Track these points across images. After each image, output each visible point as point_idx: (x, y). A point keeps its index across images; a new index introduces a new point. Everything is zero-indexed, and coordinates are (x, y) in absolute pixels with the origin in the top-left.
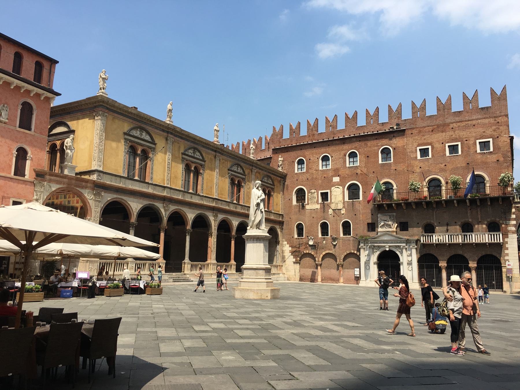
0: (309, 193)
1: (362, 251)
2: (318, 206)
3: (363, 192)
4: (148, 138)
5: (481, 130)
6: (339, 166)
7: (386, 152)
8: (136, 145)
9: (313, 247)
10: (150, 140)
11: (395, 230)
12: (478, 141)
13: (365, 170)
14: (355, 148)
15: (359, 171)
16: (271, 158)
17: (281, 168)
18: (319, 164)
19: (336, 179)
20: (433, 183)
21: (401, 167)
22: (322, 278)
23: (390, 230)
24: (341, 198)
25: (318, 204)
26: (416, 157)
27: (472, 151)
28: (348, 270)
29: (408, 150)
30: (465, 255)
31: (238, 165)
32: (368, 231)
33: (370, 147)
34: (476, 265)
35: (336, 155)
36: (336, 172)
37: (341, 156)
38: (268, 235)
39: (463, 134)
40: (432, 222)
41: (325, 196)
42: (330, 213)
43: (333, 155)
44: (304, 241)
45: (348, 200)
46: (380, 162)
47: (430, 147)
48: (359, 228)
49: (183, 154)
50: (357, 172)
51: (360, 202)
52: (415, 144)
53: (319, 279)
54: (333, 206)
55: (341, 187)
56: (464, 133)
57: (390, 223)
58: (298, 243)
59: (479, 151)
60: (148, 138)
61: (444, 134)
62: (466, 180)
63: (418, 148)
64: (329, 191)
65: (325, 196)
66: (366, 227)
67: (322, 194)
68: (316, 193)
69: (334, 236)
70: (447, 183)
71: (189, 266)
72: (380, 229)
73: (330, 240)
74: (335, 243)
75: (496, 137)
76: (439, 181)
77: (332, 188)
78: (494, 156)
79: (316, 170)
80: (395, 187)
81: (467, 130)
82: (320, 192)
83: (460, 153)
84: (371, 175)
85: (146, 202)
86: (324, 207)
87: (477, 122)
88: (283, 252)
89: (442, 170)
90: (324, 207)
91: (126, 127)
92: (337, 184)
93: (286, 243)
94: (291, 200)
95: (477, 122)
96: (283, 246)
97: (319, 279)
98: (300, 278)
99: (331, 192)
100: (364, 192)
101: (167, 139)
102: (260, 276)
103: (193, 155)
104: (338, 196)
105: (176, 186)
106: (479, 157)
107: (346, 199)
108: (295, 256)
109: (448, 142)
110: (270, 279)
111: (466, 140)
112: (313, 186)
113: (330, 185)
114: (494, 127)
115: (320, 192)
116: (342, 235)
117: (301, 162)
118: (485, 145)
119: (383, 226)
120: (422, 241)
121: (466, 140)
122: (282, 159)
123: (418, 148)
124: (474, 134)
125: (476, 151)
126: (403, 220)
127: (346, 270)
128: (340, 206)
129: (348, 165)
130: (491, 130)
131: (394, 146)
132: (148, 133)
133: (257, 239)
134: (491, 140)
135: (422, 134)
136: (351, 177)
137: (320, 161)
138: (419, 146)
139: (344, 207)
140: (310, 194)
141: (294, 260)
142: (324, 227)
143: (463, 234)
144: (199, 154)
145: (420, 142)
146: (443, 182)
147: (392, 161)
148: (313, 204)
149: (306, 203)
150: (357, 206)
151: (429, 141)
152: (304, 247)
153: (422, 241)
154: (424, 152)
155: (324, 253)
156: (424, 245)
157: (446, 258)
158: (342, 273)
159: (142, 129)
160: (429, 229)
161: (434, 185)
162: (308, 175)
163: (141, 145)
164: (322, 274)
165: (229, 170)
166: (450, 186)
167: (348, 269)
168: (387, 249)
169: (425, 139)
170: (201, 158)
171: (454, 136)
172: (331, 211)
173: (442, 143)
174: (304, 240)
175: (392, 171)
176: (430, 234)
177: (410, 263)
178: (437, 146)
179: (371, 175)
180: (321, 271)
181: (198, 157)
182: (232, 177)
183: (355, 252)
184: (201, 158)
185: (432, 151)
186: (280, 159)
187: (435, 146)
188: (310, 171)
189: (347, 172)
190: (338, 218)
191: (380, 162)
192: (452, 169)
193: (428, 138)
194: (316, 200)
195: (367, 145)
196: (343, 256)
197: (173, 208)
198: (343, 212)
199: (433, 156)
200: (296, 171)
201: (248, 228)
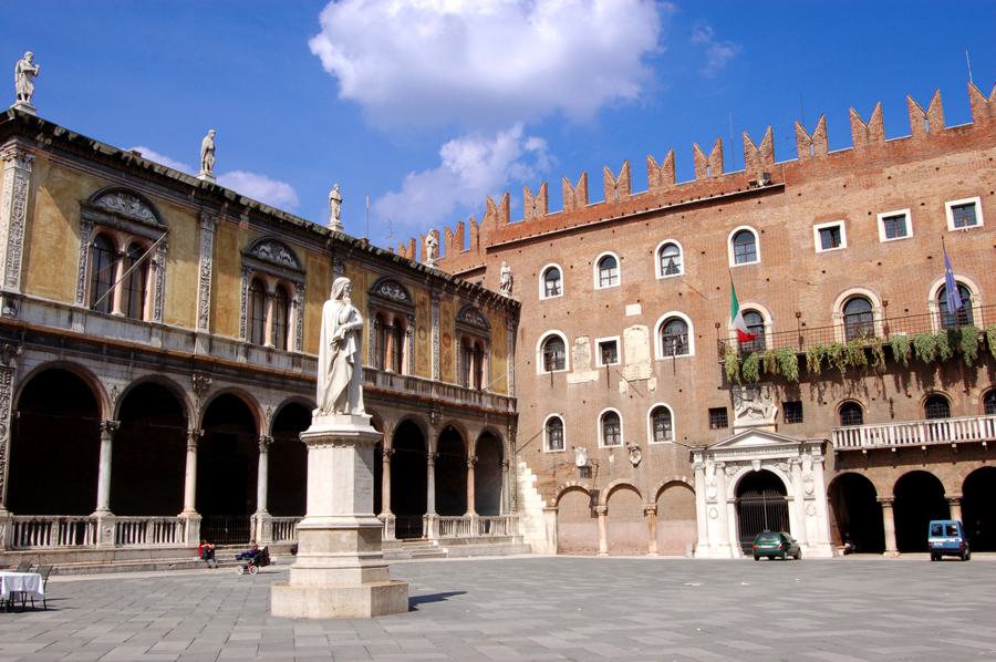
0: (572, 344)
1: (699, 473)
2: (594, 376)
3: (695, 335)
4: (146, 215)
5: (954, 178)
6: (637, 278)
7: (743, 238)
8: (113, 232)
9: (586, 471)
10: (153, 221)
11: (772, 421)
12: (948, 205)
13: (698, 285)
14: (674, 235)
15: (684, 289)
16: (483, 270)
17: (506, 291)
18: (592, 276)
19: (634, 310)
20: (852, 309)
21: (777, 274)
22: (608, 543)
23: (762, 422)
24: (644, 353)
25: (594, 369)
26: (813, 249)
27: (937, 228)
28: (671, 523)
29: (793, 234)
30: (935, 473)
31: (394, 283)
32: (711, 427)
33: (708, 231)
34: (960, 495)
35: (629, 253)
36: (633, 293)
37: (643, 255)
38: (372, 430)
39: (915, 189)
40: (857, 397)
41: (608, 349)
42: (622, 390)
43: (624, 255)
44: (566, 458)
45: (662, 358)
46: (732, 264)
47: (841, 223)
48: (690, 422)
49: (245, 255)
50: (681, 291)
51: (689, 359)
52: (810, 219)
53: (603, 547)
54: (629, 373)
55: (645, 328)
56: (917, 187)
57: (760, 406)
58: (551, 464)
59: (951, 226)
60: (146, 215)
61: (872, 191)
62: (928, 295)
64: (617, 338)
65: (608, 349)
66: (706, 416)
67: (602, 344)
68: (588, 346)
69: (633, 444)
70: (885, 304)
71: (269, 527)
72: (736, 424)
73: (624, 453)
74: (636, 461)
75: (989, 192)
76: (866, 299)
77: (626, 331)
78: (987, 236)
79: (588, 292)
80: (768, 321)
81: (922, 181)
83: (910, 232)
84: (712, 296)
85: (140, 373)
86: (609, 378)
87: (944, 160)
88: (516, 486)
89: (873, 276)
90: (609, 378)
91: (86, 186)
92: (637, 320)
93: (524, 464)
94: (531, 363)
95: (944, 160)
97: (603, 547)
98: (558, 547)
99: (622, 339)
100: (699, 336)
101: (199, 219)
102: (345, 550)
103: (271, 256)
104: (640, 347)
105: (226, 332)
107: (659, 354)
108: (545, 496)
109: (882, 211)
110: (381, 557)
111: (923, 204)
112: (581, 329)
113: (623, 323)
114: (982, 171)
115: (598, 341)
116: (651, 441)
117: (551, 275)
118: (964, 212)
119: (745, 413)
120: (835, 445)
121: (923, 204)
122: (509, 269)
123: (816, 228)
124: (938, 190)
125: (946, 228)
127: (665, 523)
128: (645, 372)
129: (658, 276)
130: (976, 177)
131: (761, 225)
132: (146, 203)
133: (338, 440)
134: (977, 200)
135: (821, 194)
136: (665, 302)
137: (596, 269)
138: (818, 220)
139: (654, 374)
140: (574, 348)
141: (544, 504)
142: (610, 419)
143: (927, 422)
144: (288, 256)
145: (819, 213)
146: (877, 303)
147: (759, 260)
148: (583, 370)
149: (567, 368)
150: (683, 370)
151: (840, 211)
152: (566, 472)
153: (835, 445)
155: (611, 486)
156: (843, 457)
157: (892, 482)
158: (654, 529)
159: (129, 194)
160: (851, 413)
162: (568, 305)
163: (130, 233)
164: (607, 533)
165: (369, 294)
166: (893, 311)
167: (668, 519)
168: (757, 469)
169: (829, 206)
170: (294, 265)
171: (894, 195)
172: (623, 386)
173: (870, 213)
174: (565, 455)
175: (761, 284)
176: (852, 428)
177: (809, 498)
178: (859, 219)
179: (712, 296)
180: (607, 528)
181: (285, 262)
182: (378, 309)
183: (684, 480)
184: (294, 265)
185: (847, 233)
186: (503, 269)
187: (853, 220)
188: (574, 294)
189: (657, 293)
190: (642, 401)
191: (732, 264)
192: (895, 272)
193: (841, 201)
194: (589, 360)
195: (700, 226)
196: (656, 490)
197: (218, 385)
198: (652, 384)
199: (849, 243)
200: (542, 296)
201: (315, 412)
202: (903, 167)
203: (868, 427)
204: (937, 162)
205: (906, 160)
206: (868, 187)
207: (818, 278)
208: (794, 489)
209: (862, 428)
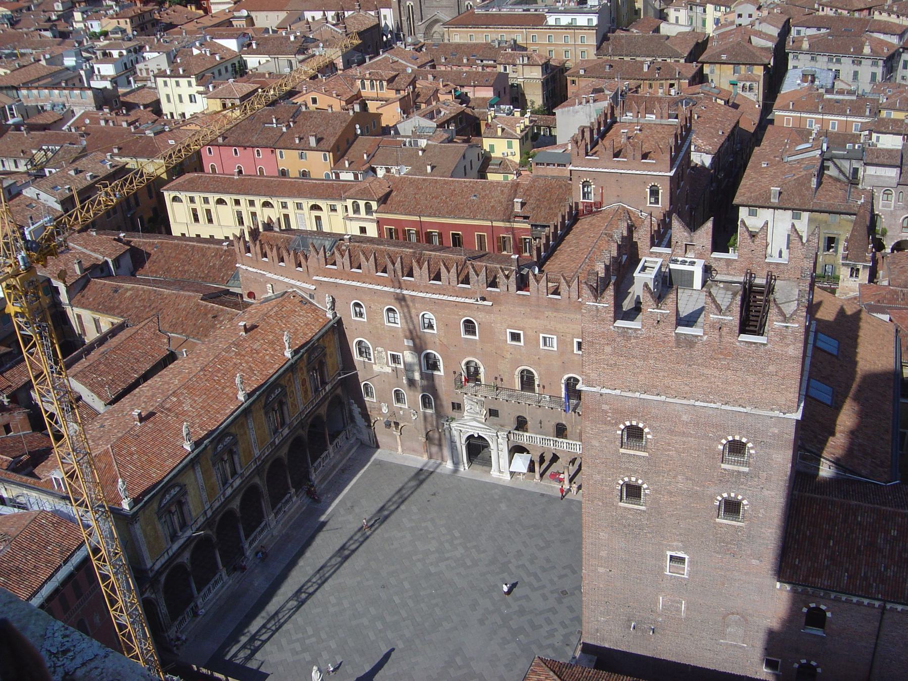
4: (177, 489)
7: (470, 327)
13: (445, 341)
14: (430, 310)
15: (437, 340)
63: (508, 331)
72: (465, 413)
82: (389, 352)
88: (351, 411)
96: (350, 404)
106: (576, 358)
112: (378, 341)
123: (508, 331)
126: (492, 407)
154: (515, 337)
161: (527, 381)
178: (530, 332)
202: (555, 314)
203: (528, 434)
204: (572, 316)
205: (557, 310)
206: (536, 318)
207: (508, 356)
208: (493, 446)
209: (525, 434)
